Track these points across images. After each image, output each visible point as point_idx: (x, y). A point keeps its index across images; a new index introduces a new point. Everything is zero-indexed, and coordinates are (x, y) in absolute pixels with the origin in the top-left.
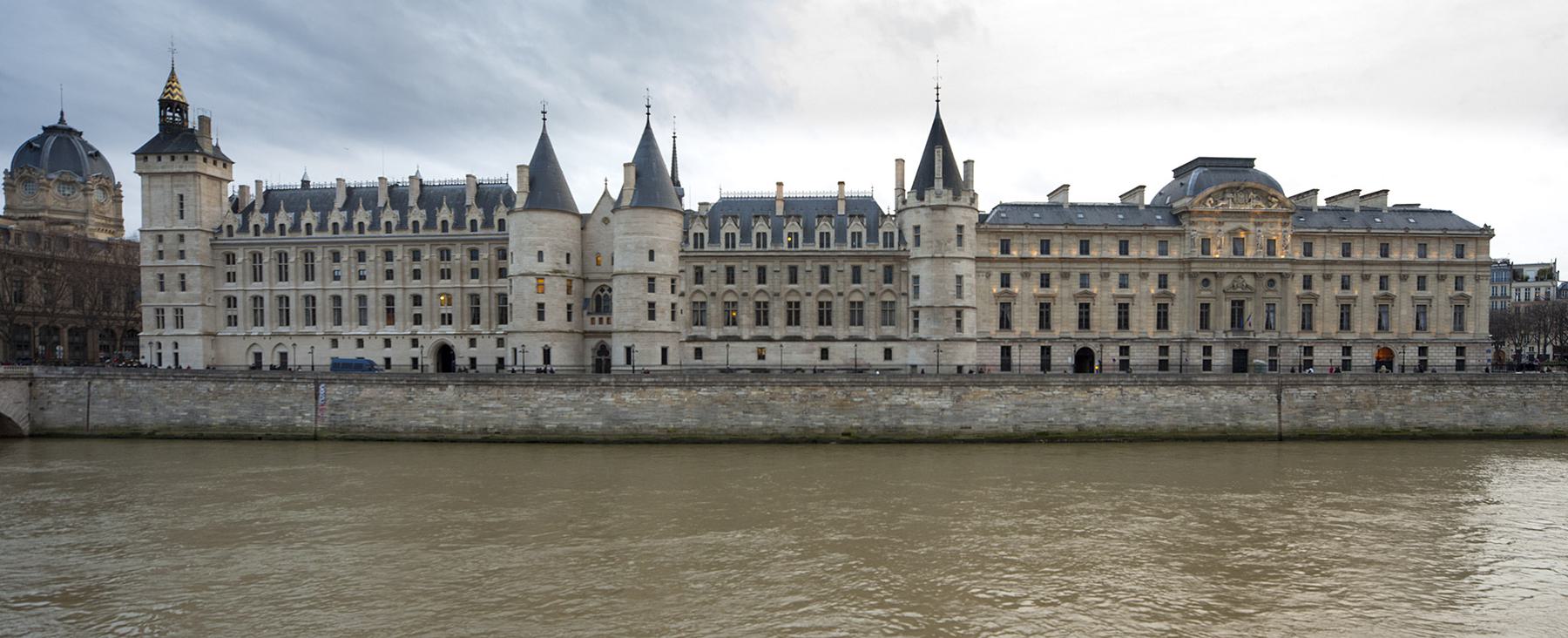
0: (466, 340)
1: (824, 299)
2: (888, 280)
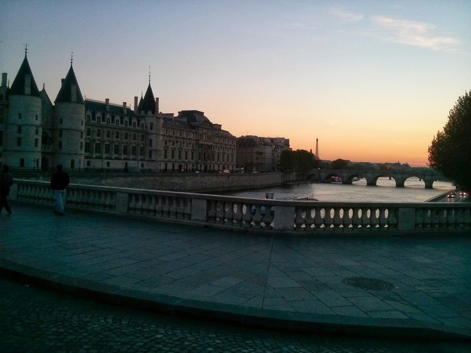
1: (126, 145)
2: (142, 140)
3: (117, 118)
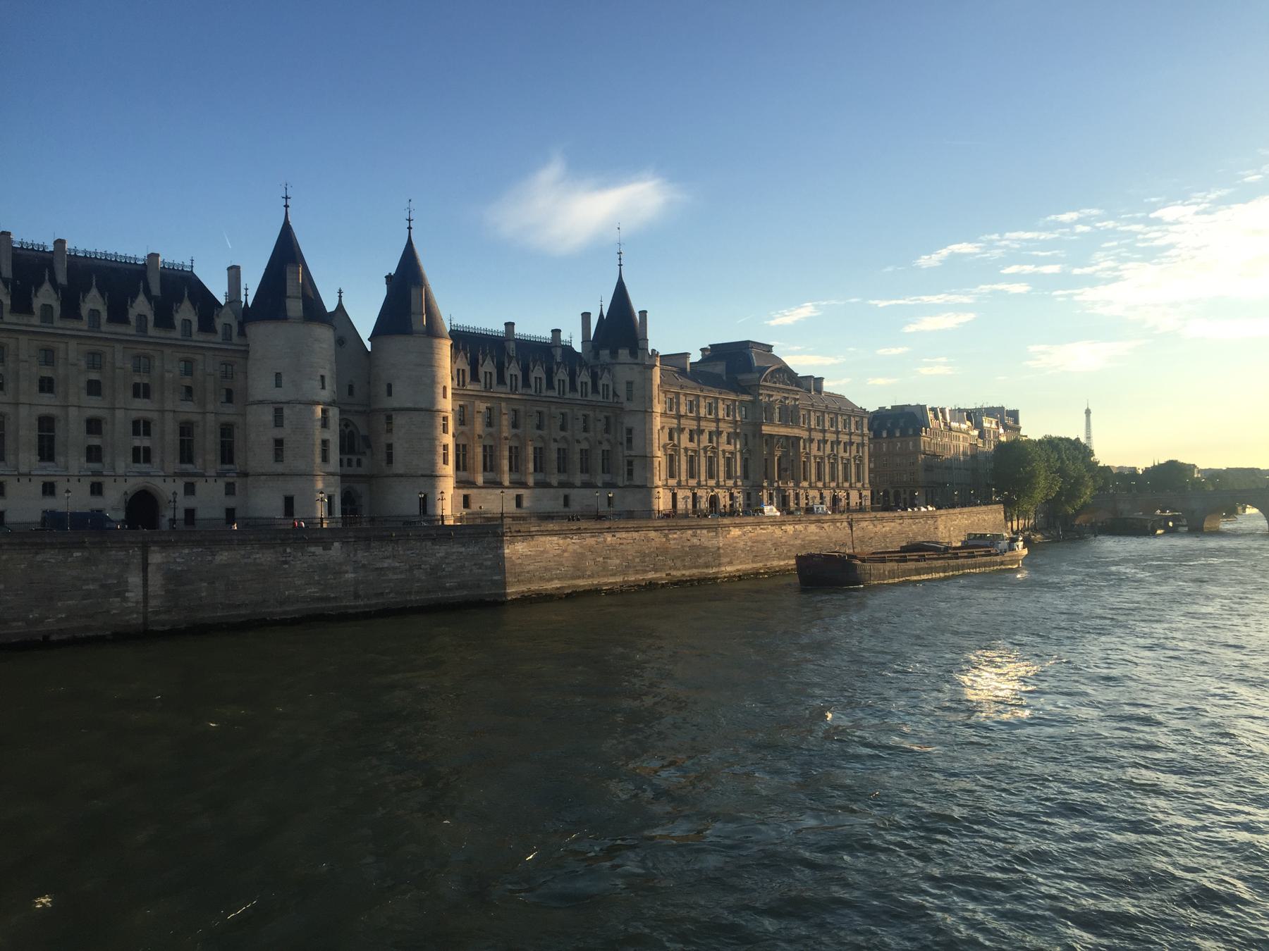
0: (179, 485)
1: (565, 446)
2: (607, 431)
3: (538, 372)
